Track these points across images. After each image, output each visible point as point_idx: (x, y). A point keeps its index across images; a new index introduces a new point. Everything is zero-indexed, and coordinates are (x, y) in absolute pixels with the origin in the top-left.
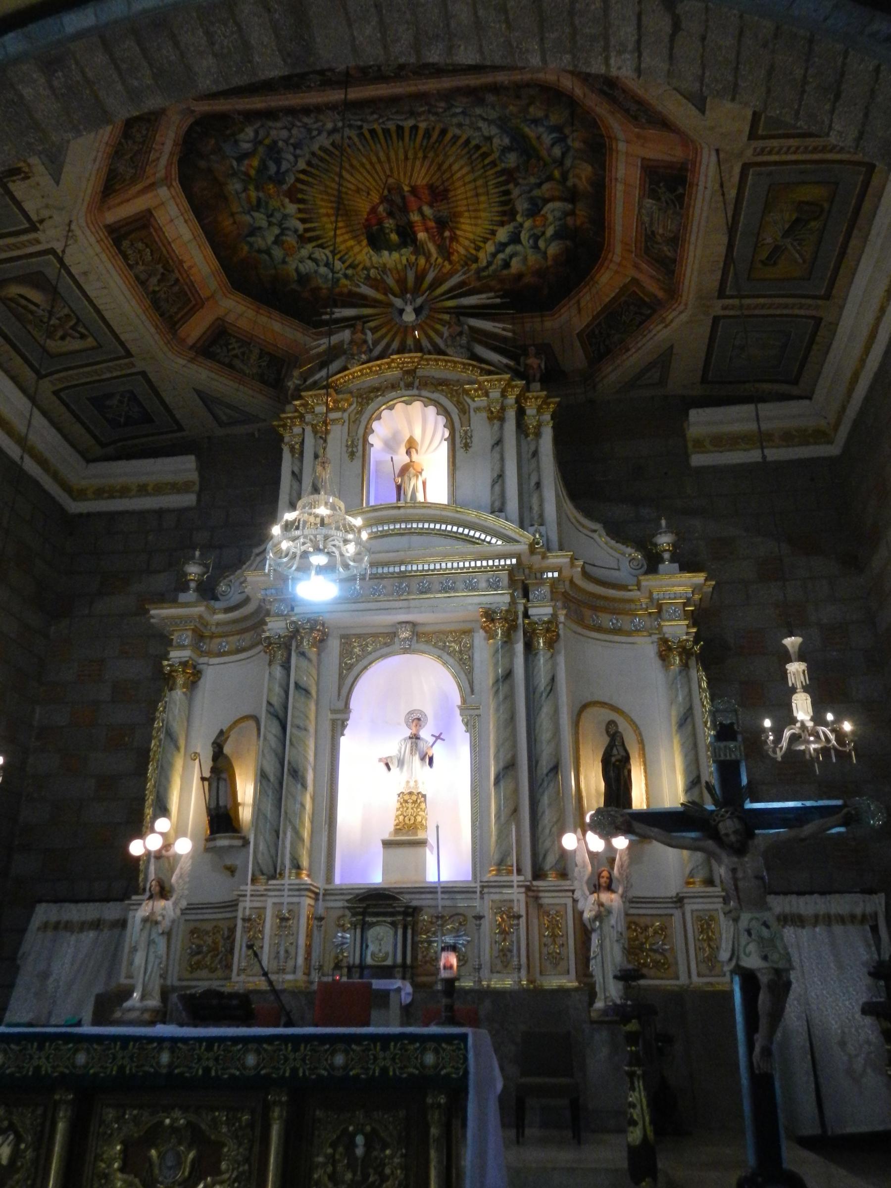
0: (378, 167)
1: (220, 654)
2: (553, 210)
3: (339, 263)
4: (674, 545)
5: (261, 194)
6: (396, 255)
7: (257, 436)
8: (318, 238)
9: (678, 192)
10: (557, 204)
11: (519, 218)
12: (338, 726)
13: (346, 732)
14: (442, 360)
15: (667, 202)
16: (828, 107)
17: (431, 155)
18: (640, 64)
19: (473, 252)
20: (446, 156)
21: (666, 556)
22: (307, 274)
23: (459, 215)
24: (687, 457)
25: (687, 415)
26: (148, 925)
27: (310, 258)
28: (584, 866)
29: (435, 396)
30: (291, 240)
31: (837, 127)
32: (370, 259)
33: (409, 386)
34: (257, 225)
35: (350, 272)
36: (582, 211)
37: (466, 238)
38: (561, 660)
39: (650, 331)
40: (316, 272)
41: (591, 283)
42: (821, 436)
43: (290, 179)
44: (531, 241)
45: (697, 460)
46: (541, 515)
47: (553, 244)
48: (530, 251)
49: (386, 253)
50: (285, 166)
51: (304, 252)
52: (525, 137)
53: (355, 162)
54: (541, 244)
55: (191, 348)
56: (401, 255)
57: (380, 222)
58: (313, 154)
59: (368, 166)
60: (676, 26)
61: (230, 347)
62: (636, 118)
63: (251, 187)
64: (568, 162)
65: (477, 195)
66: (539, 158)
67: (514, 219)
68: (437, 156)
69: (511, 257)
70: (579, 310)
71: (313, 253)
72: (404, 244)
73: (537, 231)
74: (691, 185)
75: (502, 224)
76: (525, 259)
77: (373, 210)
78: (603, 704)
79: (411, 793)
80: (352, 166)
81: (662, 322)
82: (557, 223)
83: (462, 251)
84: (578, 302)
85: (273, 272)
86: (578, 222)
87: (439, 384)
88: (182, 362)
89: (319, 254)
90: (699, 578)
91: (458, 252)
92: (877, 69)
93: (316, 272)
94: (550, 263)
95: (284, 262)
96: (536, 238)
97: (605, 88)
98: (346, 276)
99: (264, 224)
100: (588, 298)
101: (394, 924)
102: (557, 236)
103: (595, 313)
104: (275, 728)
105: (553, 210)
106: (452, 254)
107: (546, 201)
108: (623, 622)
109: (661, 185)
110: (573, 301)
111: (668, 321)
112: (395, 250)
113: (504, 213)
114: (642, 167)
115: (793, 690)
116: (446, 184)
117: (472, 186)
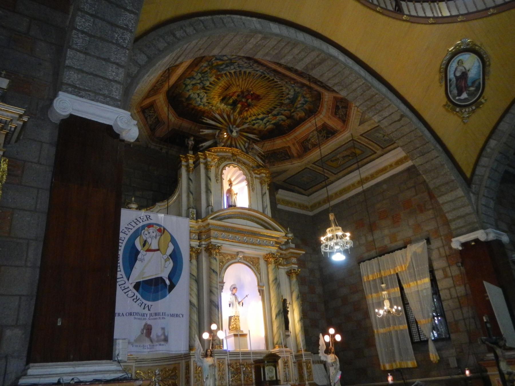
0: (252, 83)
2: (280, 117)
3: (206, 100)
5: (209, 71)
6: (226, 106)
7: (132, 146)
8: (208, 90)
9: (328, 135)
10: (283, 117)
11: (270, 115)
13: (223, 291)
14: (247, 155)
15: (322, 136)
16: (418, 155)
17: (269, 89)
18: (382, 120)
19: (248, 117)
20: (273, 92)
22: (192, 98)
23: (256, 106)
26: (211, 368)
27: (198, 94)
28: (323, 346)
29: (243, 167)
30: (199, 86)
31: (417, 160)
32: (217, 104)
33: (234, 160)
34: (195, 77)
35: (206, 104)
36: (288, 122)
37: (250, 113)
39: (285, 163)
40: (196, 99)
41: (273, 141)
42: (305, 207)
43: (223, 72)
44: (266, 122)
47: (271, 125)
48: (263, 124)
49: (223, 104)
50: (228, 68)
51: (198, 92)
52: (297, 98)
53: (248, 79)
54: (268, 124)
55: (141, 107)
56: (227, 107)
57: (233, 95)
58: (240, 71)
59: (249, 82)
60: (399, 120)
61: (151, 111)
62: (336, 114)
63: (208, 67)
64: (298, 110)
65: (268, 104)
66: (294, 105)
67: (268, 115)
68: (270, 90)
69: (257, 123)
70: (263, 146)
71: (201, 93)
72: (231, 105)
73: (270, 120)
74: (335, 136)
75: (264, 114)
76: (260, 125)
77: (235, 93)
79: (237, 316)
80: (246, 79)
81: (291, 162)
82: (277, 121)
83: (245, 115)
84: (264, 144)
85: (180, 91)
86: (283, 124)
87: (244, 164)
88: (135, 111)
89: (202, 94)
91: (244, 115)
92: (437, 157)
93: (196, 99)
94: (265, 130)
95: (188, 91)
96: (268, 121)
97: (340, 107)
98: (204, 105)
99: (197, 78)
100: (269, 144)
102: (274, 124)
103: (269, 150)
105: (280, 117)
106: (242, 114)
107: (282, 114)
109: (325, 131)
110: (263, 143)
111: (293, 163)
112: (227, 105)
113: (268, 112)
114: (323, 124)
115: (384, 299)
116: (263, 97)
117: (269, 101)
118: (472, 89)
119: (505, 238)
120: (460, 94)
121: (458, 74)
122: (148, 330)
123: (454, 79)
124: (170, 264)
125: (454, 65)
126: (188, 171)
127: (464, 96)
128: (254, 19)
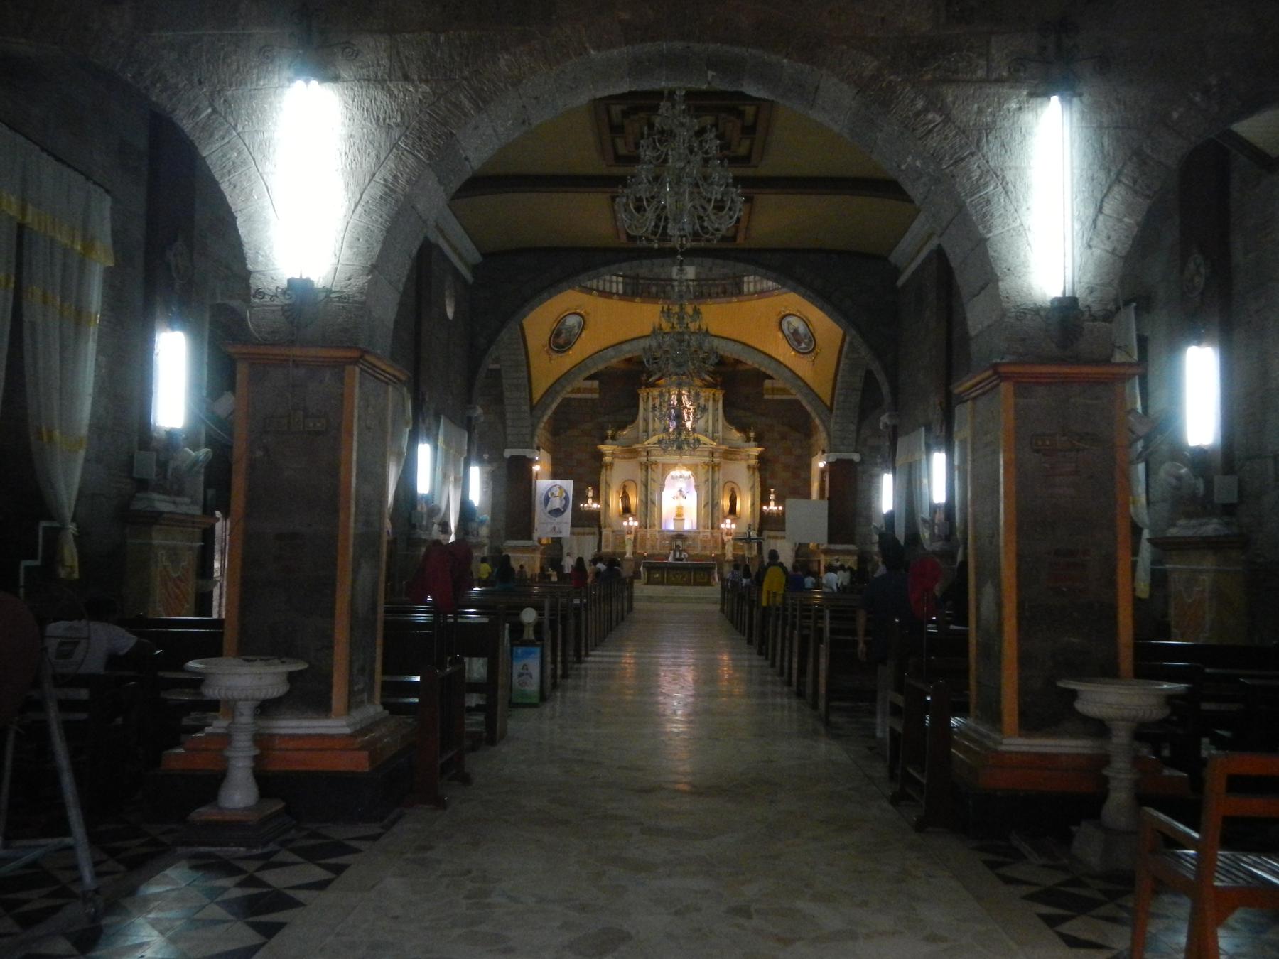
1: (619, 458)
4: (755, 435)
12: (662, 487)
21: (752, 439)
24: (763, 395)
25: (763, 380)
38: (721, 472)
45: (766, 397)
46: (718, 430)
78: (731, 482)
90: (760, 449)
101: (682, 541)
104: (643, 488)
108: (738, 457)
118: (806, 340)
119: (856, 457)
120: (800, 345)
121: (792, 331)
122: (554, 528)
123: (790, 335)
124: (564, 502)
125: (785, 325)
126: (643, 401)
127: (803, 345)
128: (609, 349)
